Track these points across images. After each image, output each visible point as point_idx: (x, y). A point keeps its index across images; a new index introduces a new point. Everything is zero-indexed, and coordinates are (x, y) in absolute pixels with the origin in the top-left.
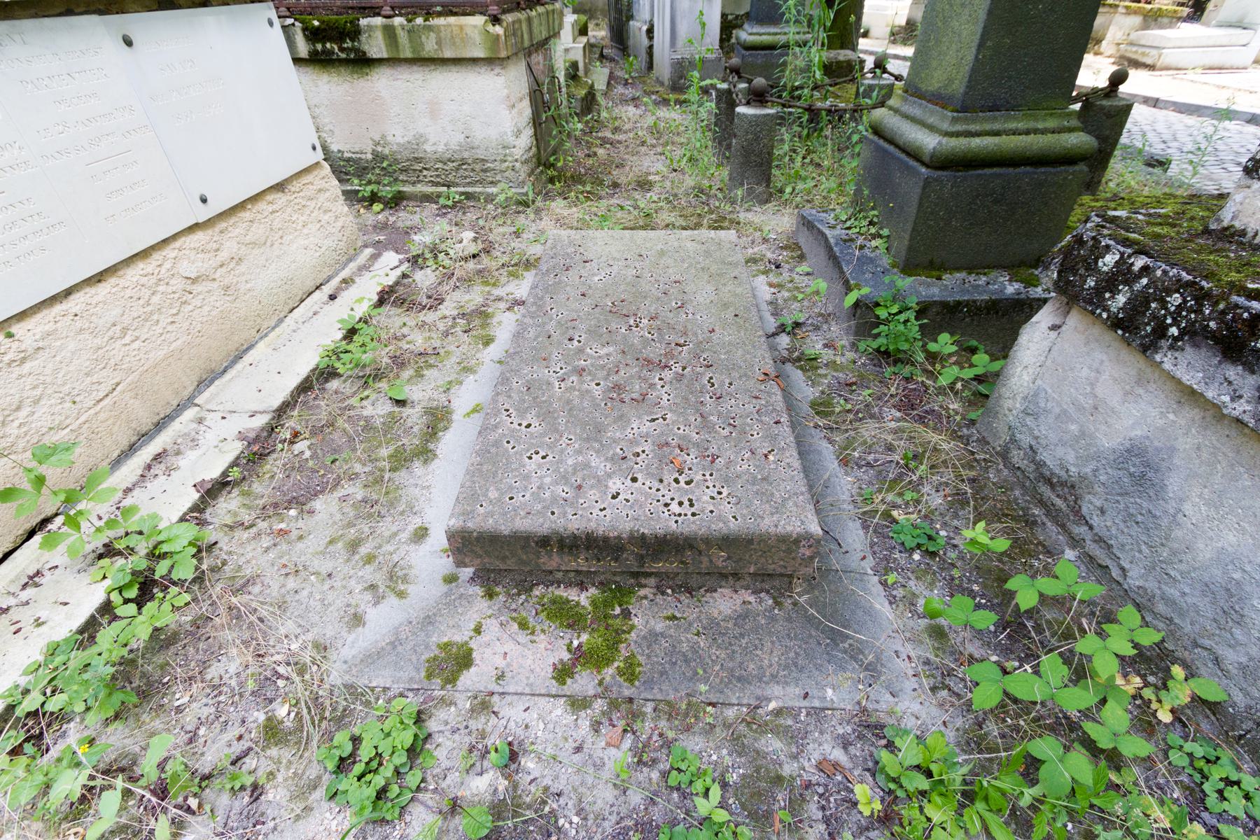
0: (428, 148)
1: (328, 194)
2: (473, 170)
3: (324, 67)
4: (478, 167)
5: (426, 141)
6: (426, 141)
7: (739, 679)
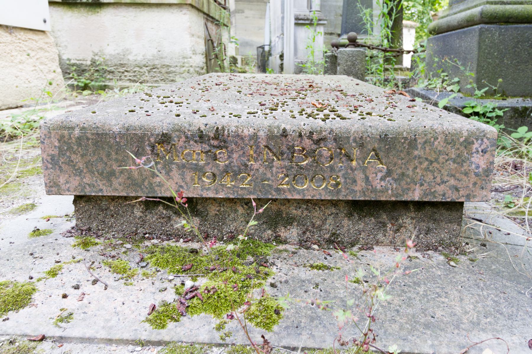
0: (131, 57)
1: (47, 54)
2: (160, 72)
3: (70, 8)
4: (164, 70)
5: (131, 53)
6: (131, 53)
7: (427, 326)
